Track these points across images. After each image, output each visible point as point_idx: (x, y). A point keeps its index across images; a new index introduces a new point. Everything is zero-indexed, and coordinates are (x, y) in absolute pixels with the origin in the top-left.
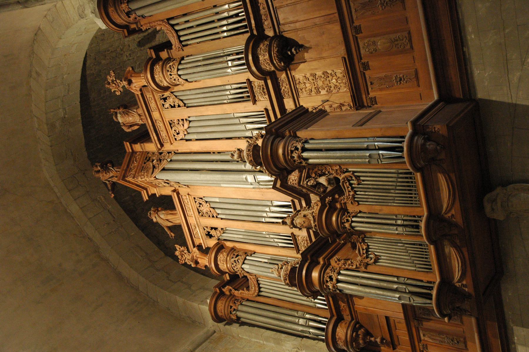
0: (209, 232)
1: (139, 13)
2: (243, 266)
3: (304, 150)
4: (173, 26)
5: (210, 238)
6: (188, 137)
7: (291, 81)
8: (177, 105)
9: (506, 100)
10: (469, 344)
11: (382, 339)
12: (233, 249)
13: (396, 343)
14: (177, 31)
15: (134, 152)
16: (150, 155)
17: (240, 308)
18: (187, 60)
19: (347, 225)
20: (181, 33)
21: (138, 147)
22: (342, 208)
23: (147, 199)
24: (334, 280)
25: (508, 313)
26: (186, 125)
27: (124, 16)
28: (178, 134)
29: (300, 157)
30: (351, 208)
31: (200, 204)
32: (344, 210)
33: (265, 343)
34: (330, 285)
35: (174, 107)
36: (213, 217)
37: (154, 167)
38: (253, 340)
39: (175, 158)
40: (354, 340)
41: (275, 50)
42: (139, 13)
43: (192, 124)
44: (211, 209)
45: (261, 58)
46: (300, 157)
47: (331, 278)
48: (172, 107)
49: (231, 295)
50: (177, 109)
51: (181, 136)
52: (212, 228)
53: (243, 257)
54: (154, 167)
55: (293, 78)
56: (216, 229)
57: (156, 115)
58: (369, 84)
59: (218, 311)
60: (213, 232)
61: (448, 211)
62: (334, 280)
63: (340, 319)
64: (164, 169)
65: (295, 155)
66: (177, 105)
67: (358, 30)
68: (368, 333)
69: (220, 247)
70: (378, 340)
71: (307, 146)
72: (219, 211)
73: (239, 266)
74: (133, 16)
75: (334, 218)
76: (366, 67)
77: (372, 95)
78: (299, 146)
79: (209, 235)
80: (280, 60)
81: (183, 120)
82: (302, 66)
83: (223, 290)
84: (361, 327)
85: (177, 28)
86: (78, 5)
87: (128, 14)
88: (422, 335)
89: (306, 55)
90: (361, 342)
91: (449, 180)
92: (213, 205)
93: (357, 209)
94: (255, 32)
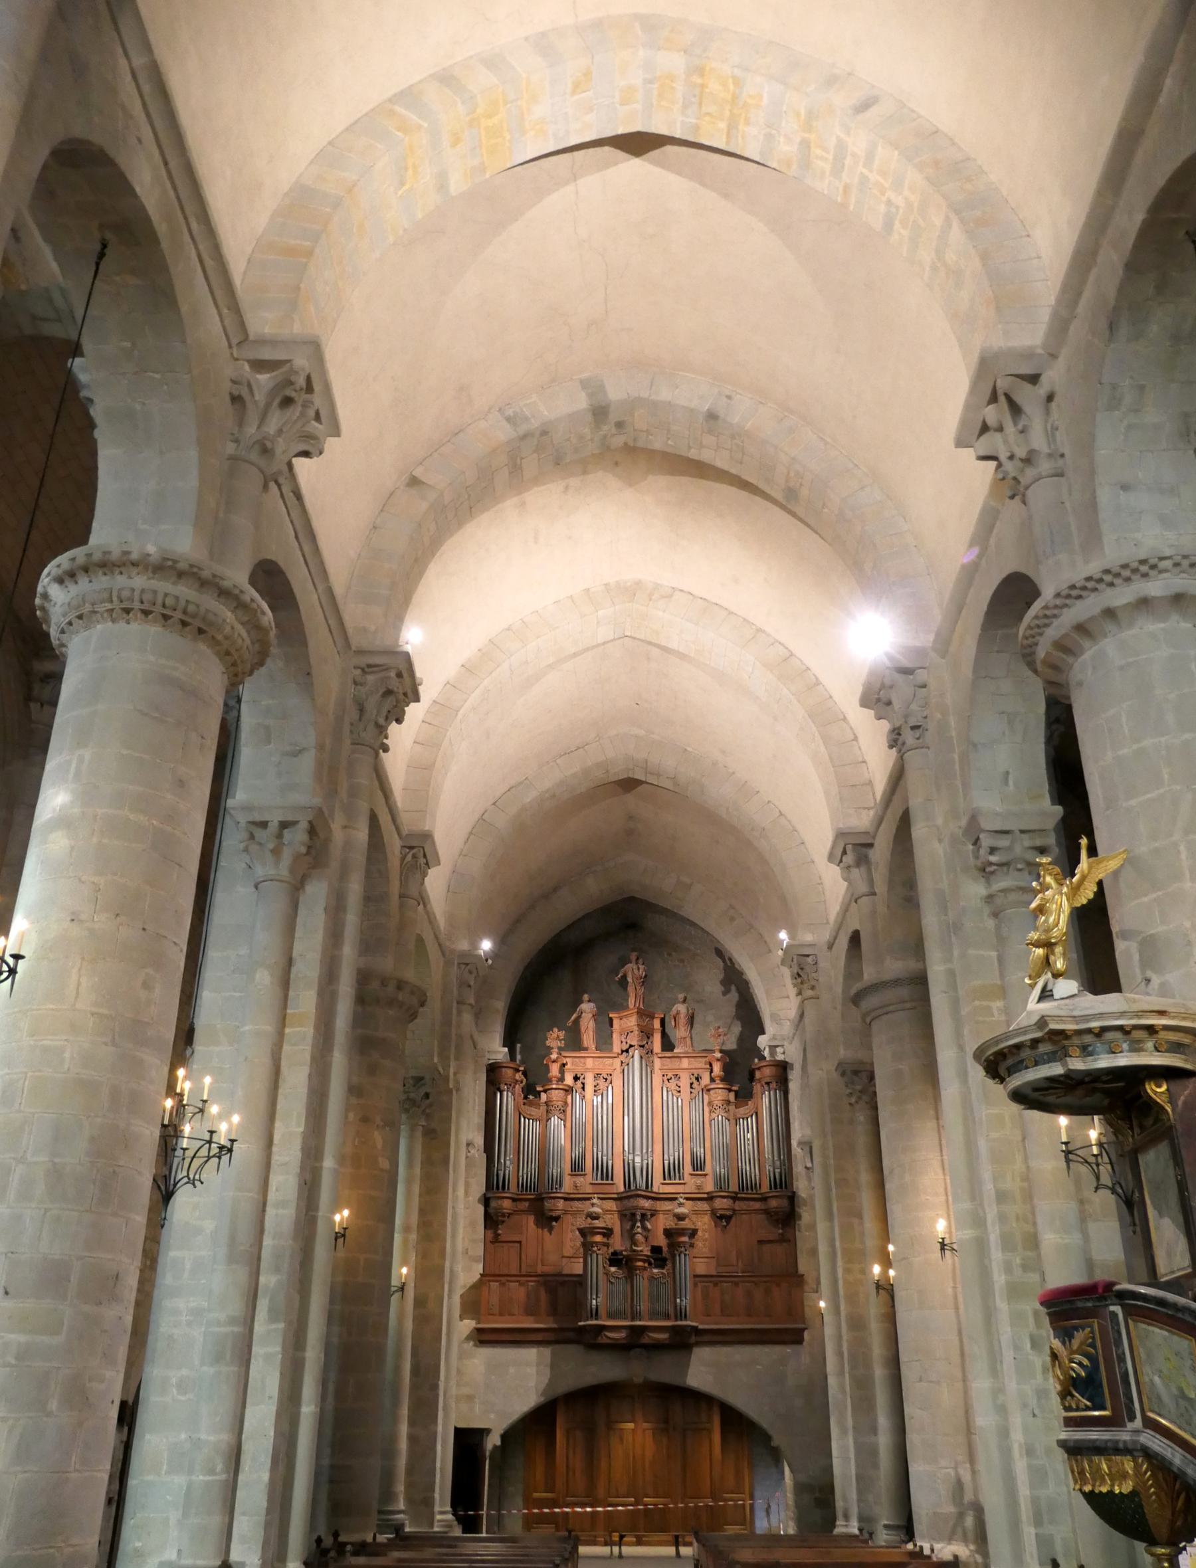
0: (579, 1078)
1: (767, 1093)
2: (556, 1117)
3: (685, 1255)
4: (752, 1116)
5: (574, 1078)
6: (665, 1089)
7: (704, 1212)
8: (693, 1091)
9: (691, 1364)
10: (531, 1318)
11: (499, 1235)
12: (566, 1103)
13: (497, 1244)
14: (747, 1119)
15: (653, 1018)
16: (651, 1038)
17: (510, 1094)
18: (727, 1122)
19: (638, 1272)
20: (745, 1122)
21: (657, 1024)
22: (645, 1267)
23: (610, 1015)
24: (598, 1252)
25: (557, 1346)
26: (675, 1093)
27: (768, 1080)
28: (668, 1080)
29: (681, 1252)
30: (646, 1274)
31: (606, 1079)
32: (645, 1269)
33: (476, 1111)
34: (595, 1249)
35: (691, 1088)
36: (595, 1091)
37: (643, 1046)
38: (476, 1098)
39: (649, 1071)
40: (503, 1215)
41: (729, 1213)
42: (767, 1093)
43: (675, 1098)
44: (601, 1091)
45: (725, 1200)
46: (681, 1252)
47: (599, 1250)
48: (692, 1084)
49: (517, 1081)
50: (689, 1089)
51: (668, 1085)
52: (583, 1084)
53: (563, 1118)
54: (643, 1046)
55: (706, 1214)
56: (583, 1088)
57: (685, 1063)
58: (706, 1284)
59: (506, 1069)
60: (579, 1083)
61: (649, 1336)
62: (598, 1252)
63: (514, 1200)
64: (641, 1057)
65: (683, 1249)
66: (693, 1091)
67: (736, 1284)
68: (503, 1222)
69: (569, 1090)
70: (500, 1232)
71: (687, 1257)
72: (600, 1098)
73: (557, 1112)
74: (766, 1088)
75: (640, 1264)
76: (716, 1284)
77: (699, 1284)
78: (687, 1252)
79: (576, 1078)
80: (721, 1215)
81: (679, 1092)
82: (713, 1224)
83: (520, 1073)
84: (508, 1217)
85: (749, 1119)
86: (782, 1017)
87: (768, 1083)
88: (532, 1284)
89: (719, 1229)
90: (500, 1218)
91: (666, 1339)
92: (605, 1093)
93: (645, 1277)
94: (739, 1195)
